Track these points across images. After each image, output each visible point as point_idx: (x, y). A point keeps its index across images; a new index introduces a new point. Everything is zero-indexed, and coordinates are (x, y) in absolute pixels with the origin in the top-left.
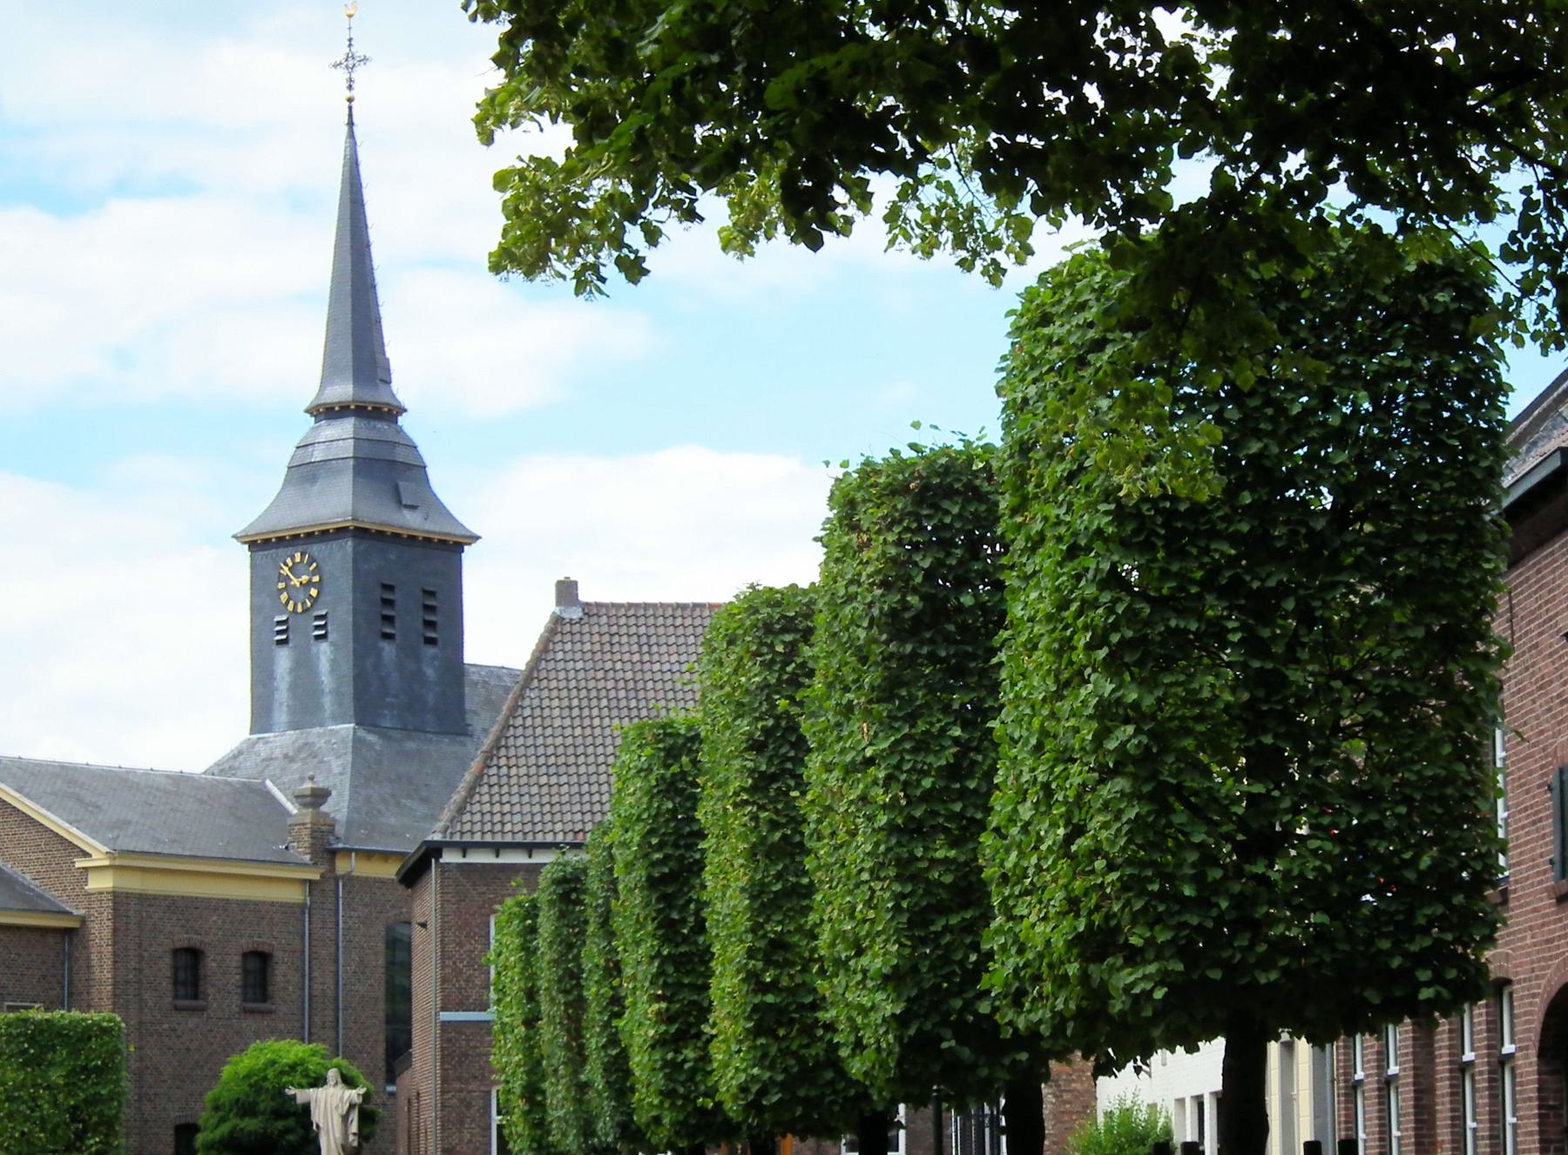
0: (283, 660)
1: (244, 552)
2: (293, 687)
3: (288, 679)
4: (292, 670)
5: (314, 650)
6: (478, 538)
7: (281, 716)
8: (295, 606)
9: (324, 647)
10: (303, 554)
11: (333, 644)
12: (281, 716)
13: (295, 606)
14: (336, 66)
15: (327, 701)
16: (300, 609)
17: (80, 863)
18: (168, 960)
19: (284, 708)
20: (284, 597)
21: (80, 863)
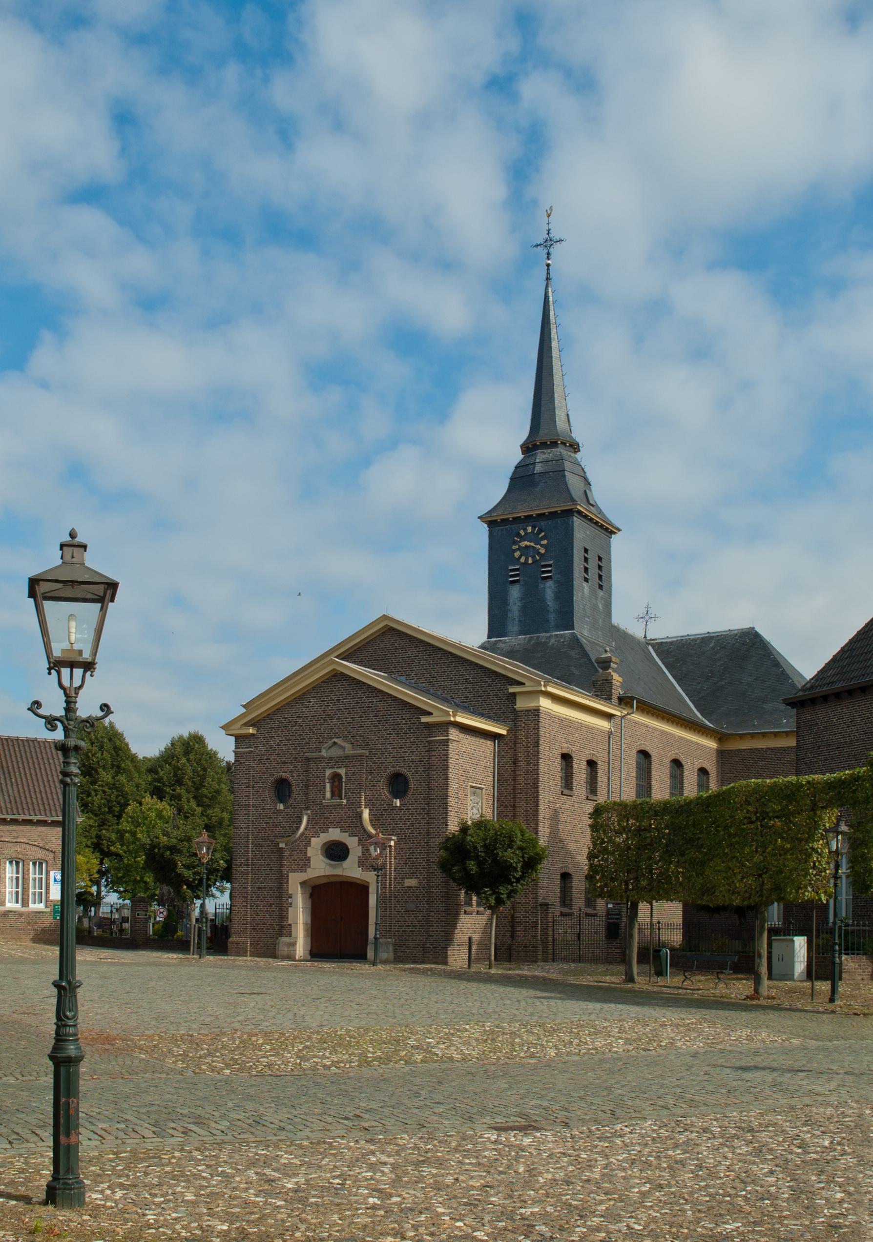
0: (515, 593)
1: (484, 528)
2: (524, 609)
3: (519, 604)
4: (522, 599)
5: (541, 586)
6: (619, 530)
7: (514, 627)
8: (527, 559)
9: (549, 584)
10: (534, 527)
11: (556, 582)
12: (514, 627)
13: (527, 559)
14: (561, 240)
15: (552, 617)
16: (530, 561)
17: (512, 690)
18: (559, 760)
19: (516, 622)
20: (517, 554)
21: (512, 690)
